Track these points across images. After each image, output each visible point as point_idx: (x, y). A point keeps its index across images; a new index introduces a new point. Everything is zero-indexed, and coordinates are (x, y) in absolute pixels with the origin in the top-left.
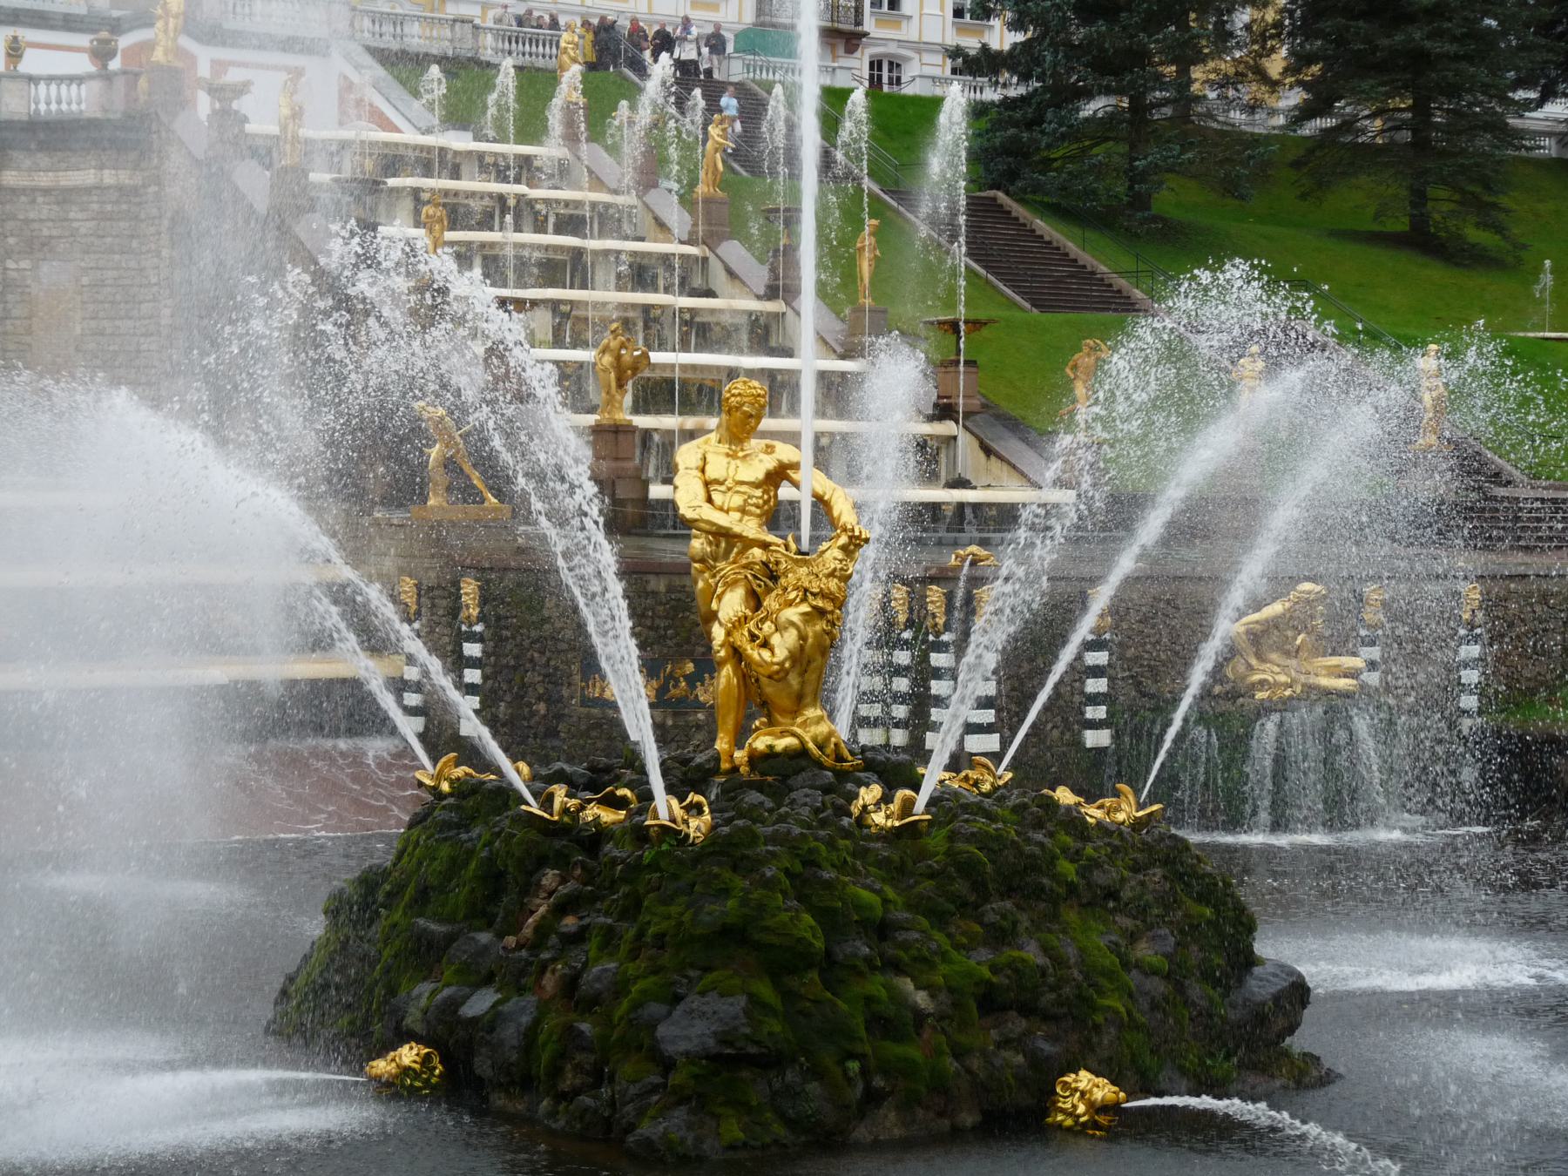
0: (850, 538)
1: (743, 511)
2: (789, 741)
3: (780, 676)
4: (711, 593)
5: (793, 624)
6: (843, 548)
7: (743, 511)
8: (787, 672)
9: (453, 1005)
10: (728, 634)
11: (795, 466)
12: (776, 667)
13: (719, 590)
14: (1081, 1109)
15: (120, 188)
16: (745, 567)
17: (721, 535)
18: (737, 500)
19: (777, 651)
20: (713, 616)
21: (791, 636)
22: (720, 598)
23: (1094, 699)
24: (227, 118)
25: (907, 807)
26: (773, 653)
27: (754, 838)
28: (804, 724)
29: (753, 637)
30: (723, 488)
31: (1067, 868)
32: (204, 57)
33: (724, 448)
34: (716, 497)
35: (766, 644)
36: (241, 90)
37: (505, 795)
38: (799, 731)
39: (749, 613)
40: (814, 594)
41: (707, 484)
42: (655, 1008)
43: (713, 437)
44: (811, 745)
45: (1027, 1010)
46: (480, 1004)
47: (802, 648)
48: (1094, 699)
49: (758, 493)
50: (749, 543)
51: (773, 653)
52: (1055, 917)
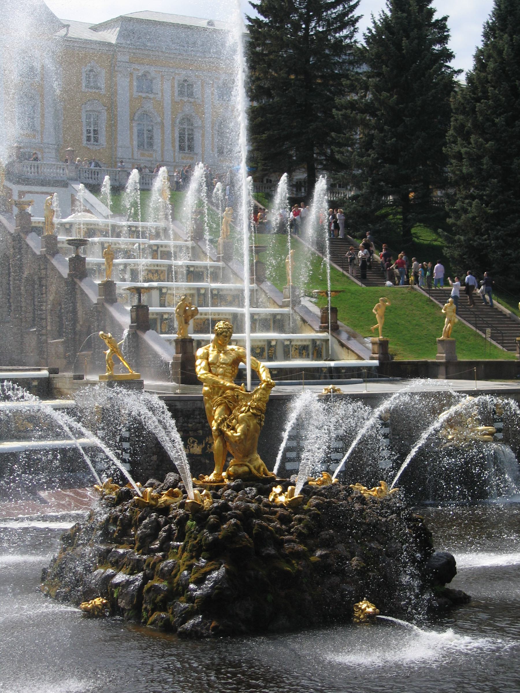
2: (246, 469)
16: (225, 398)
28: (250, 462)
35: (234, 429)
36: (29, 203)
38: (248, 464)
40: (252, 408)
41: (209, 364)
44: (253, 470)
46: (120, 578)
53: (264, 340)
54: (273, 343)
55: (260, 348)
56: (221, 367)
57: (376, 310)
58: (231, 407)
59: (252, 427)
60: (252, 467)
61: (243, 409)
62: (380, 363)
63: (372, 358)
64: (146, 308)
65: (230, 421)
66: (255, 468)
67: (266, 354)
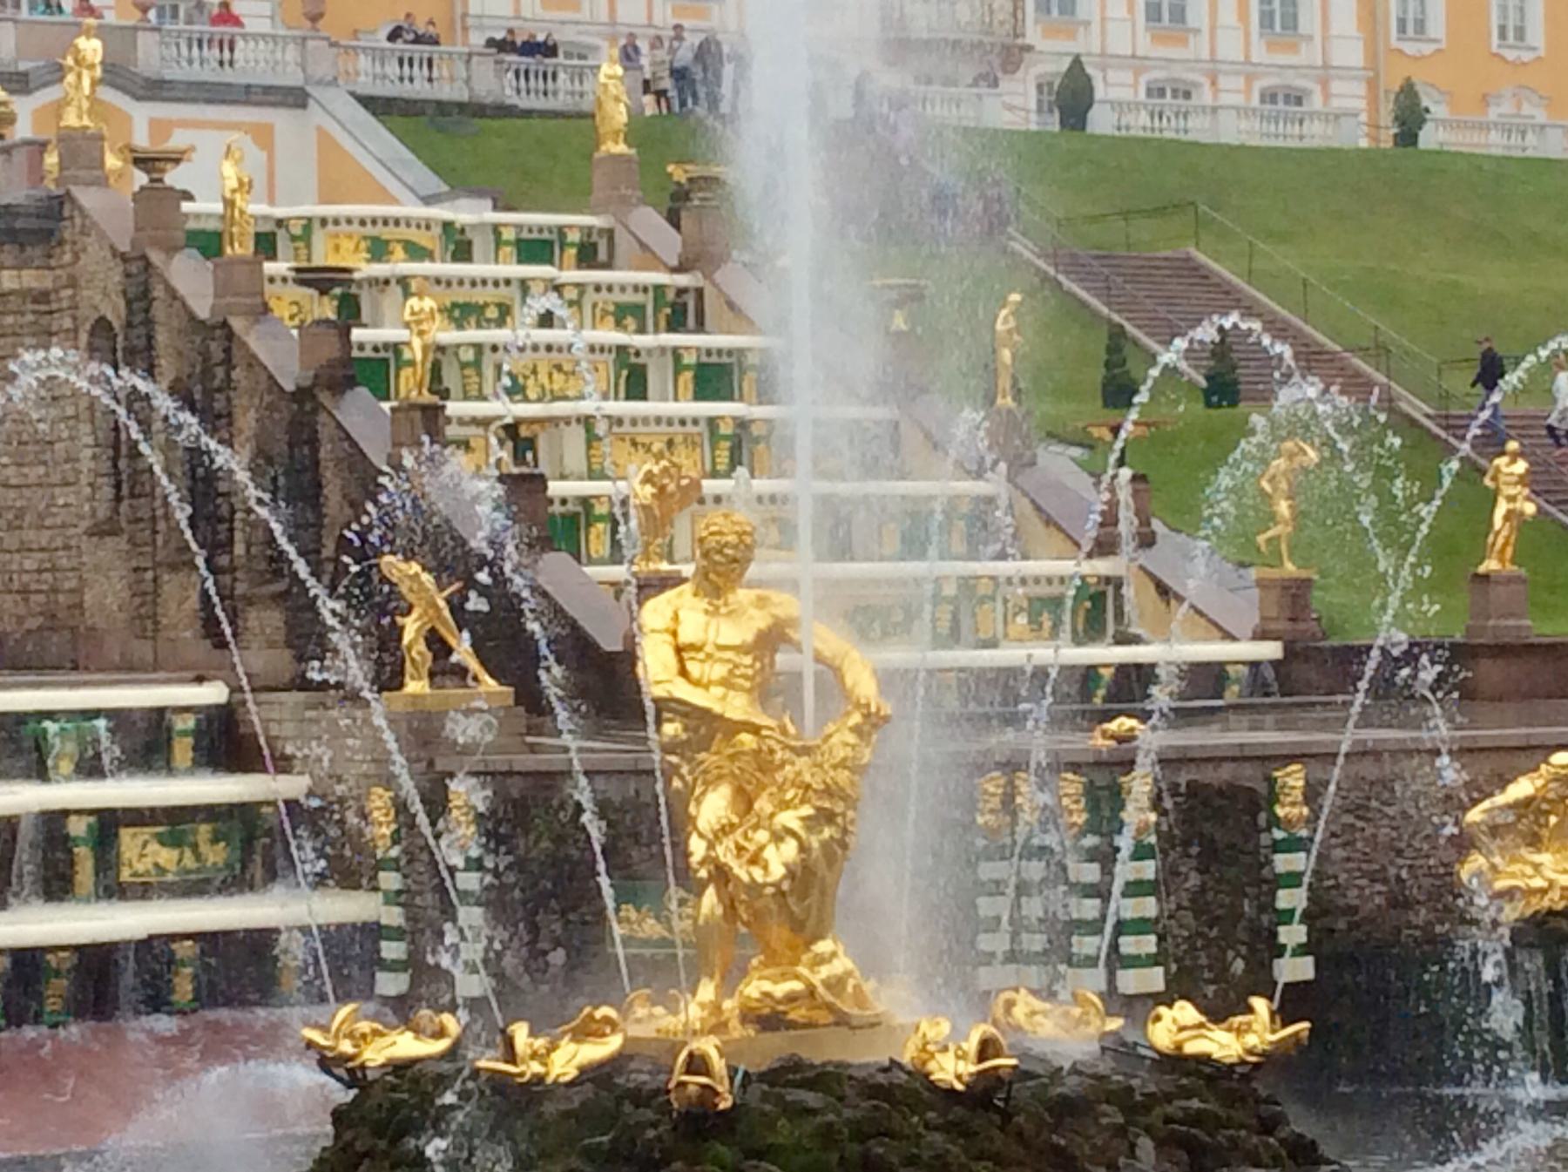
1: (726, 683)
4: (686, 796)
5: (793, 834)
6: (856, 730)
7: (726, 683)
11: (793, 622)
13: (698, 791)
15: (24, 294)
18: (719, 671)
21: (790, 849)
22: (699, 802)
24: (159, 202)
26: (765, 868)
30: (701, 656)
32: (142, 122)
33: (703, 604)
34: (691, 667)
39: (735, 820)
41: (679, 650)
43: (687, 588)
49: (748, 660)
50: (735, 727)
56: (721, 660)
60: (816, 980)
61: (789, 795)
62: (1286, 649)
63: (1261, 635)
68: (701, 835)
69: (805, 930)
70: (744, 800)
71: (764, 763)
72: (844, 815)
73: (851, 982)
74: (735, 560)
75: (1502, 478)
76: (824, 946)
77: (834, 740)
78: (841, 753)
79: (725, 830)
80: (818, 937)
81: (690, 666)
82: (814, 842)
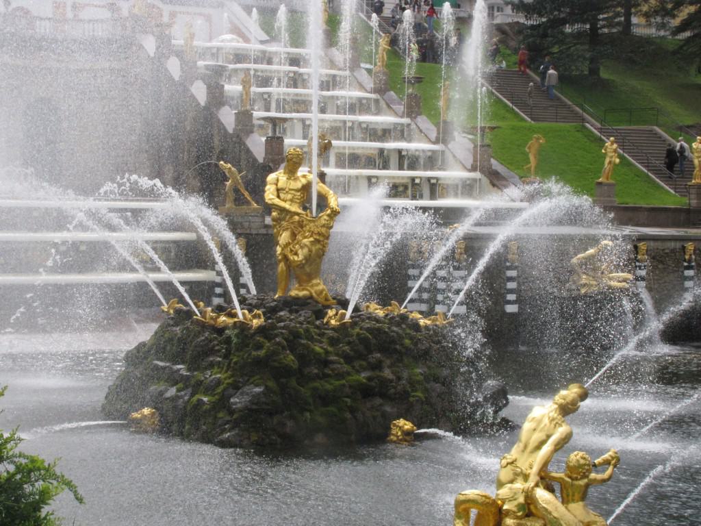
0: (332, 211)
1: (291, 200)
3: (301, 266)
5: (306, 245)
6: (329, 215)
7: (291, 200)
8: (304, 265)
9: (161, 393)
10: (282, 250)
12: (299, 263)
14: (399, 433)
16: (292, 223)
17: (282, 210)
18: (289, 196)
19: (300, 256)
20: (277, 243)
21: (306, 250)
23: (511, 291)
24: (164, 40)
25: (343, 315)
27: (276, 328)
29: (291, 251)
31: (407, 342)
33: (286, 176)
34: (282, 195)
35: (296, 254)
37: (190, 314)
38: (309, 288)
39: (290, 241)
41: (278, 190)
42: (231, 391)
44: (314, 294)
45: (383, 396)
47: (310, 255)
48: (511, 291)
49: (299, 194)
51: (298, 257)
52: (401, 361)
53: (408, 177)
54: (417, 181)
55: (403, 186)
57: (529, 148)
58: (296, 232)
59: (314, 251)
60: (313, 291)
64: (280, 140)
65: (293, 247)
66: (316, 293)
67: (409, 192)
68: (280, 246)
69: (310, 277)
70: (294, 235)
71: (301, 225)
72: (323, 241)
73: (324, 292)
74: (296, 163)
75: (608, 150)
76: (315, 281)
77: (322, 218)
78: (323, 222)
79: (288, 244)
80: (313, 279)
81: (281, 195)
82: (314, 249)
